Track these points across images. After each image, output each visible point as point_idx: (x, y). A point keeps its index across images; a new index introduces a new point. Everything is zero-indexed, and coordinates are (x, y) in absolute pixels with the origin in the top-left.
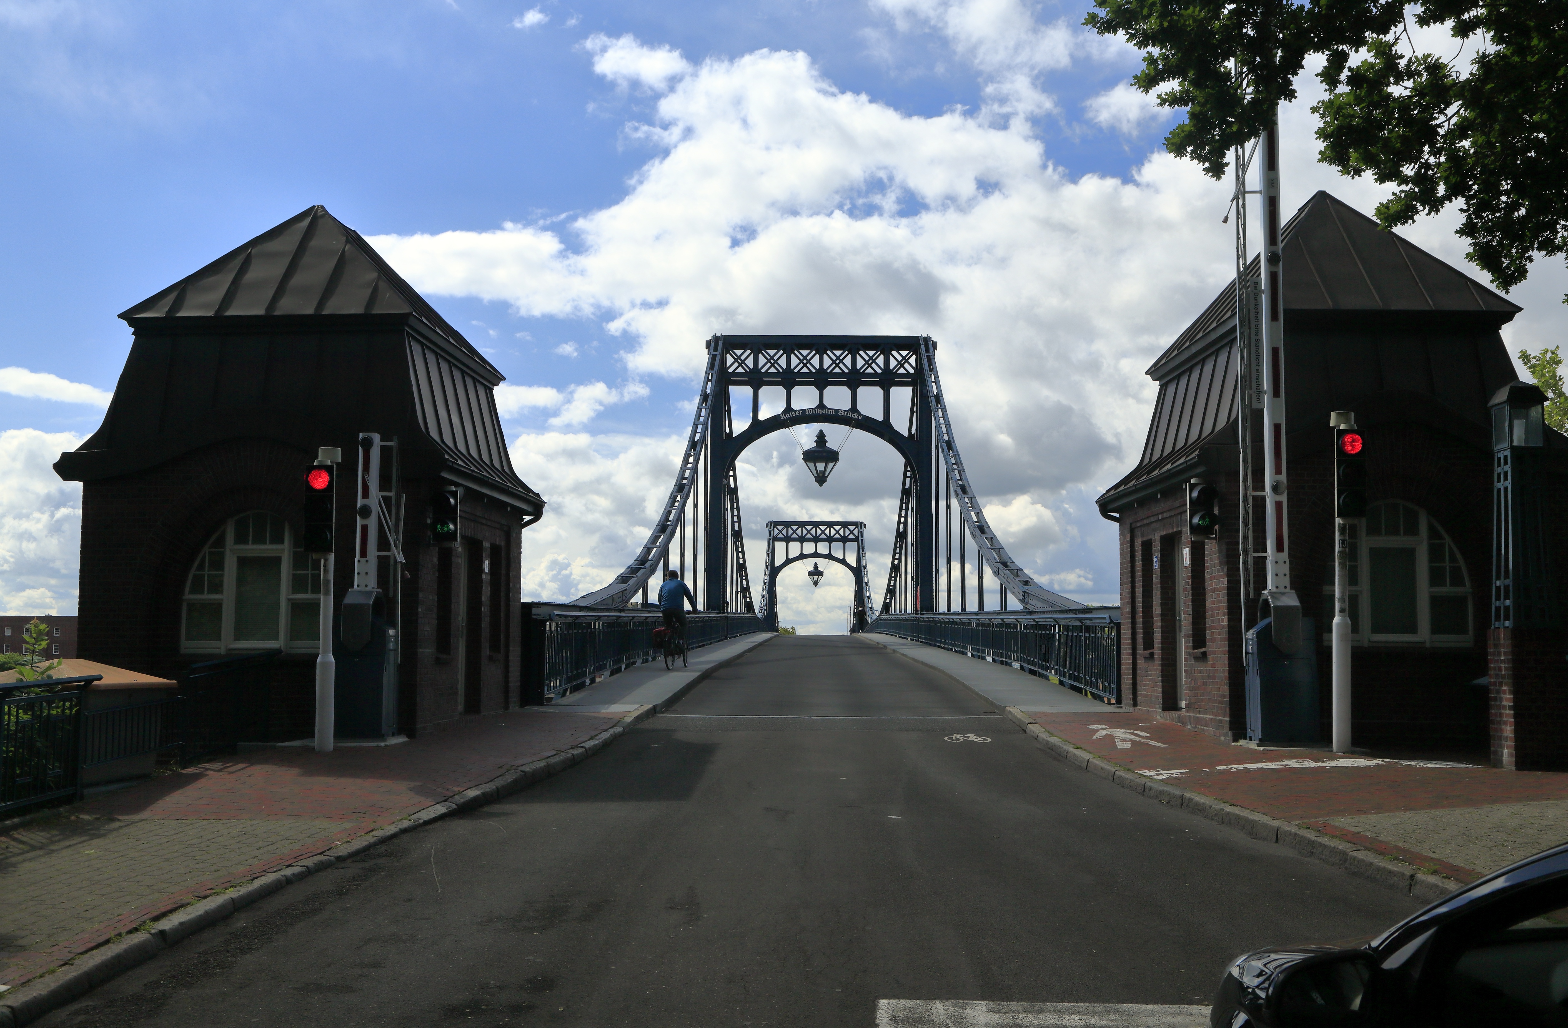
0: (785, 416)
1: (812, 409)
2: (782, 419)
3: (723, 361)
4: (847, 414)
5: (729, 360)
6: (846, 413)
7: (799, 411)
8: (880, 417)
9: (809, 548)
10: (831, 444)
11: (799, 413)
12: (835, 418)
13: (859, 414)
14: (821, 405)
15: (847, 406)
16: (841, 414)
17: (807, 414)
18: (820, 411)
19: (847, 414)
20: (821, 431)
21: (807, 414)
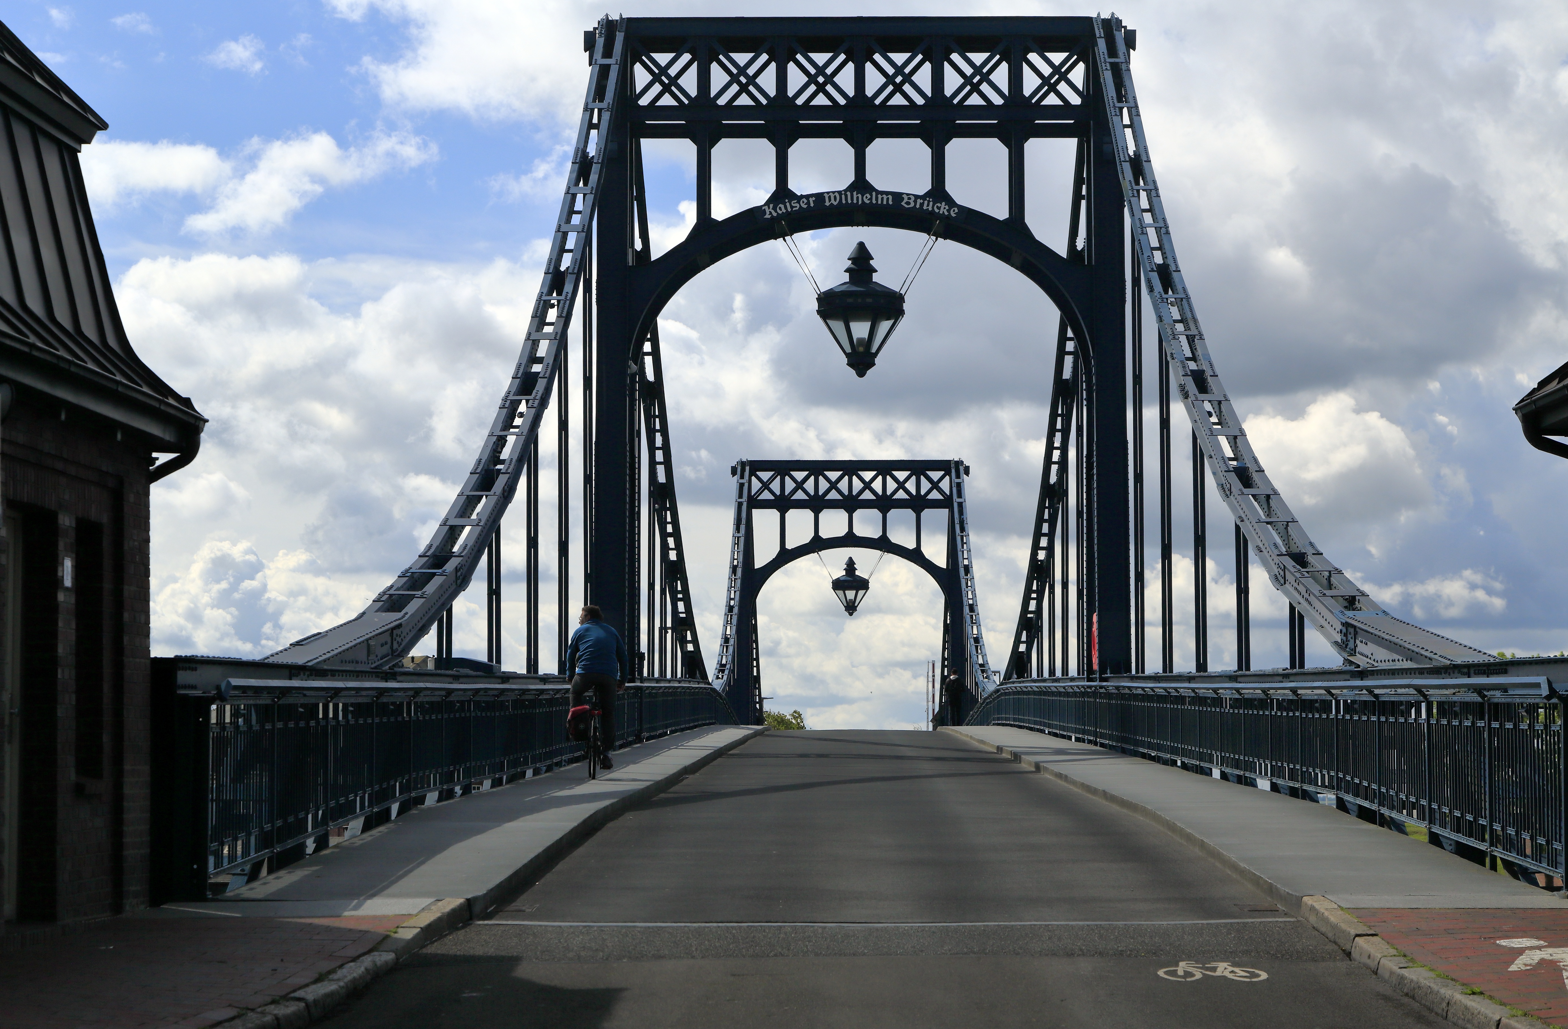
0: (775, 209)
1: (840, 192)
2: (768, 216)
3: (626, 78)
4: (922, 205)
5: (641, 76)
6: (919, 201)
7: (808, 197)
8: (1000, 211)
11: (808, 203)
14: (861, 183)
16: (908, 203)
18: (857, 198)
19: (922, 205)
20: (861, 246)
21: (827, 204)
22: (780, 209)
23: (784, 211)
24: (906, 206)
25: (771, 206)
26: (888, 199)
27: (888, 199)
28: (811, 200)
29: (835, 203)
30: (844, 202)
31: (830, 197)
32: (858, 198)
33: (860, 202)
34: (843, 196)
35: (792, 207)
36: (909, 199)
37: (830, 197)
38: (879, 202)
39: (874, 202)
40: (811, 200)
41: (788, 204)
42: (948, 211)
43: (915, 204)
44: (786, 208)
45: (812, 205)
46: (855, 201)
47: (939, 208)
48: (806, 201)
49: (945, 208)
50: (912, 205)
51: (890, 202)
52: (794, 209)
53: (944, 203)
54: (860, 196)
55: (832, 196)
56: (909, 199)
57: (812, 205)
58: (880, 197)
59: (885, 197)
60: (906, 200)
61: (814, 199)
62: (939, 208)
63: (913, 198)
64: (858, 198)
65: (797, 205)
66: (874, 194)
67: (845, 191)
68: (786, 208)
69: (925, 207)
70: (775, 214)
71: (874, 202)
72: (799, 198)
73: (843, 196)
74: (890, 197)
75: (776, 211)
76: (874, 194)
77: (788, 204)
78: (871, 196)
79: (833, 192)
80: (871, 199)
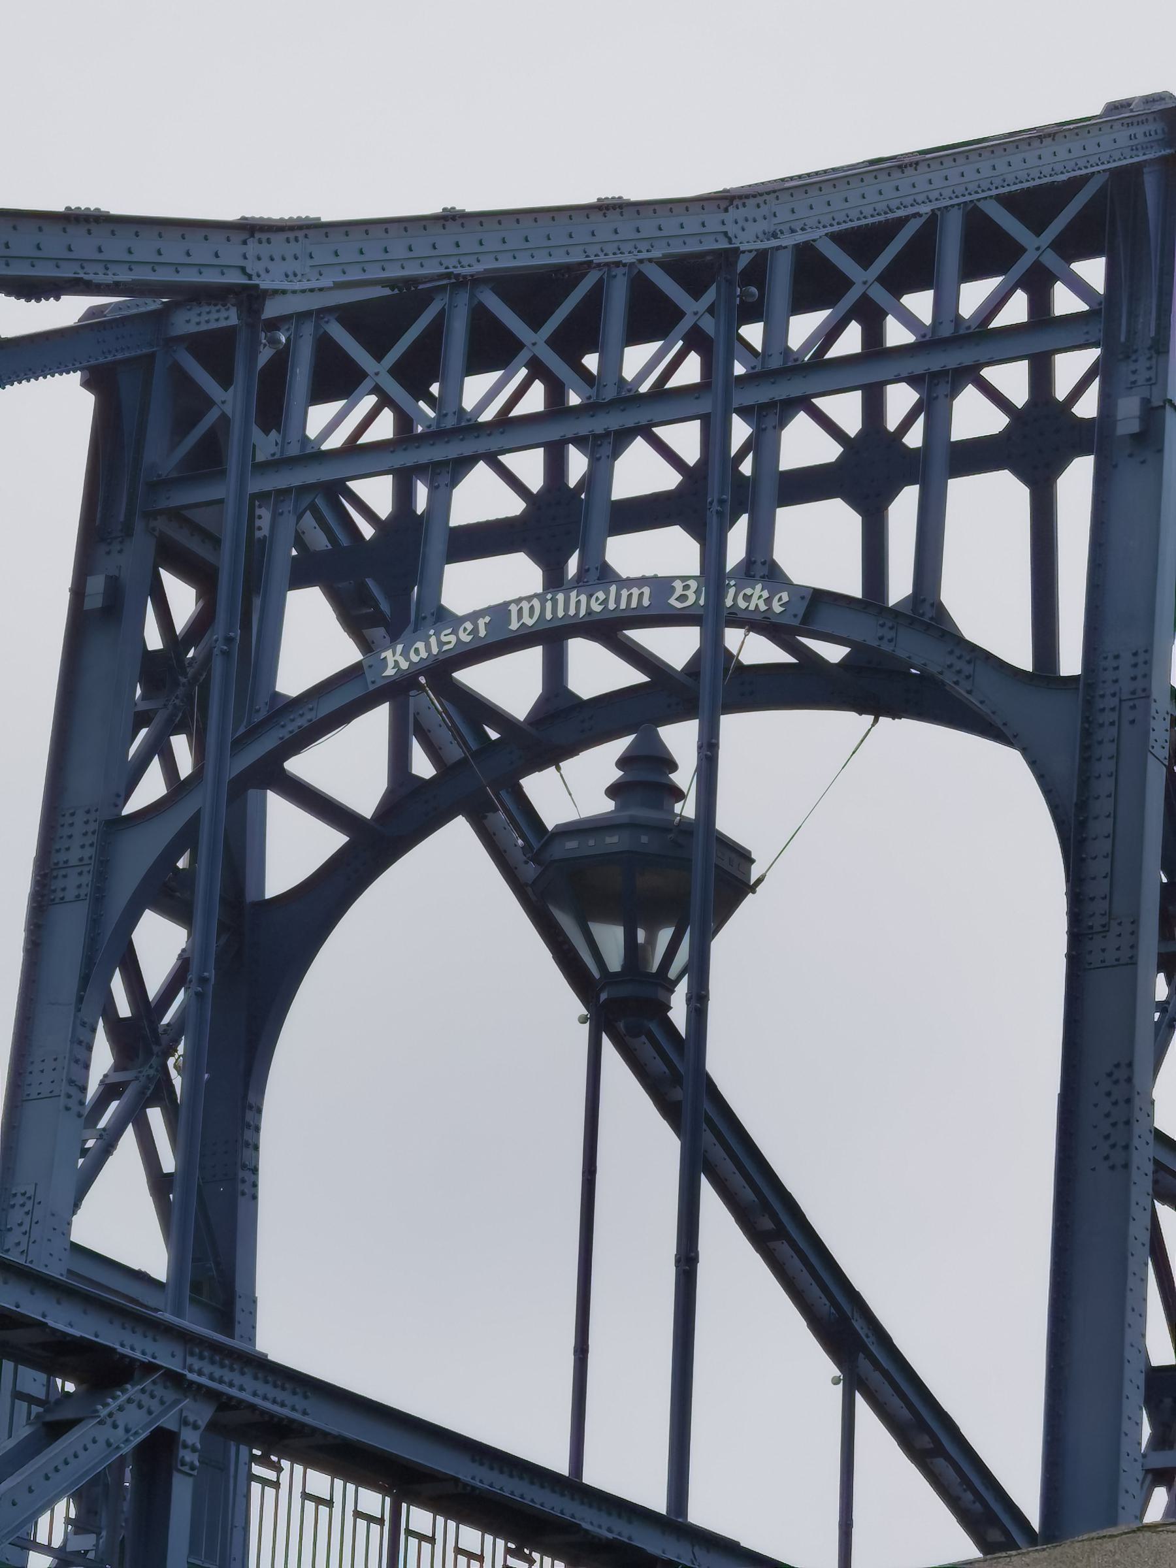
0: (405, 654)
2: (390, 672)
7: (474, 616)
11: (475, 631)
16: (683, 598)
17: (514, 625)
21: (514, 625)
22: (417, 651)
23: (424, 655)
24: (679, 605)
25: (399, 648)
26: (641, 595)
27: (641, 595)
28: (482, 623)
29: (530, 622)
30: (549, 616)
31: (520, 611)
32: (578, 602)
33: (583, 612)
34: (549, 605)
35: (441, 644)
36: (687, 587)
37: (520, 611)
38: (623, 606)
39: (612, 606)
40: (482, 623)
41: (433, 640)
42: (768, 601)
43: (698, 599)
44: (428, 647)
45: (482, 633)
46: (572, 612)
47: (747, 598)
48: (469, 626)
49: (760, 597)
51: (646, 602)
52: (446, 648)
53: (759, 587)
54: (583, 598)
55: (525, 606)
56: (687, 587)
57: (482, 633)
58: (625, 593)
59: (635, 592)
60: (679, 591)
61: (487, 619)
62: (747, 598)
64: (578, 602)
65: (453, 638)
66: (613, 589)
68: (428, 647)
70: (404, 665)
71: (612, 606)
73: (549, 605)
74: (646, 591)
75: (407, 658)
76: (613, 589)
77: (433, 640)
78: (607, 594)
80: (605, 602)
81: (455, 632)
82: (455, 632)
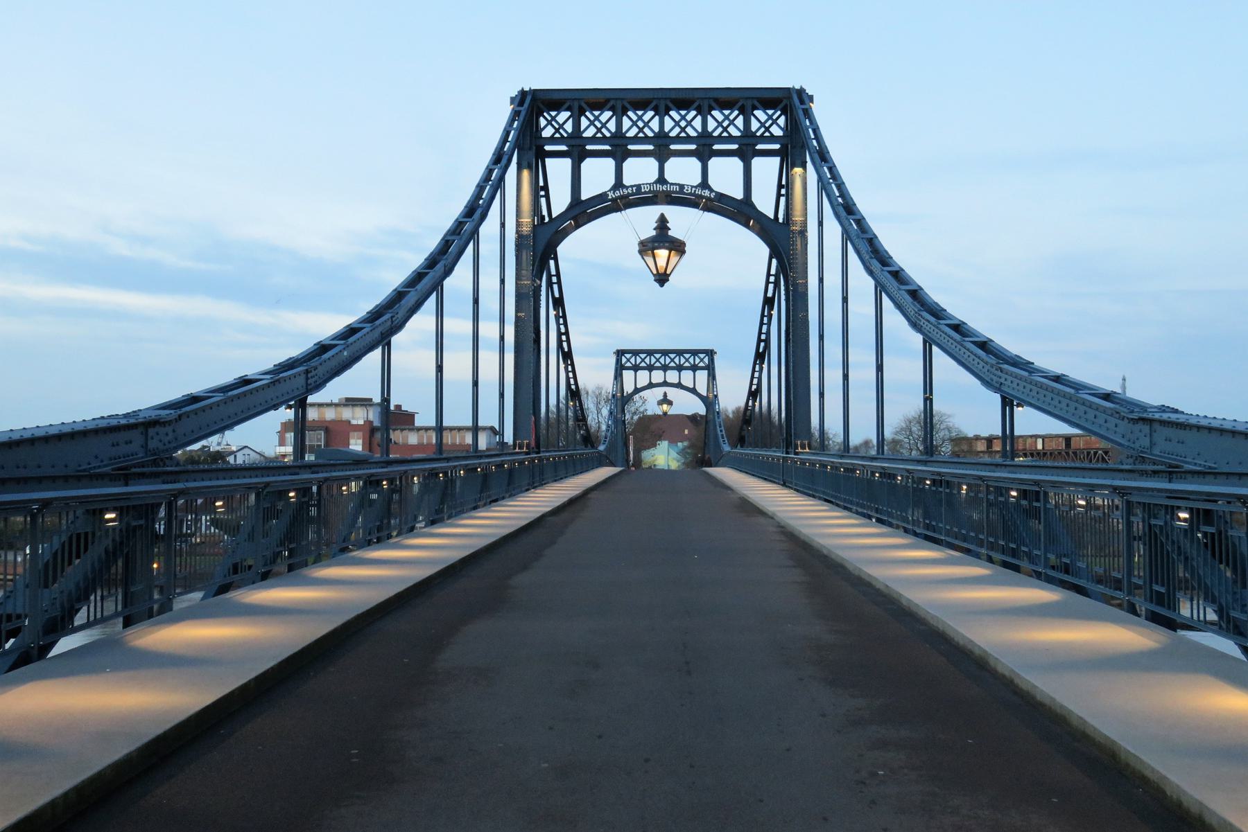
0: (614, 194)
1: (650, 184)
2: (610, 197)
4: (695, 191)
6: (694, 189)
7: (632, 186)
8: (739, 195)
9: (658, 376)
10: (675, 232)
11: (632, 190)
12: (679, 198)
13: (711, 190)
14: (661, 180)
15: (697, 180)
16: (687, 190)
18: (659, 187)
19: (695, 191)
21: (643, 190)
28: (634, 188)
35: (623, 192)
42: (710, 194)
47: (704, 193)
50: (690, 191)
58: (672, 187)
59: (675, 187)
60: (686, 188)
62: (704, 193)
63: (690, 187)
67: (653, 183)
69: (697, 193)
70: (614, 196)
72: (627, 188)
79: (647, 184)
80: (667, 188)
81: (627, 190)
82: (627, 190)
